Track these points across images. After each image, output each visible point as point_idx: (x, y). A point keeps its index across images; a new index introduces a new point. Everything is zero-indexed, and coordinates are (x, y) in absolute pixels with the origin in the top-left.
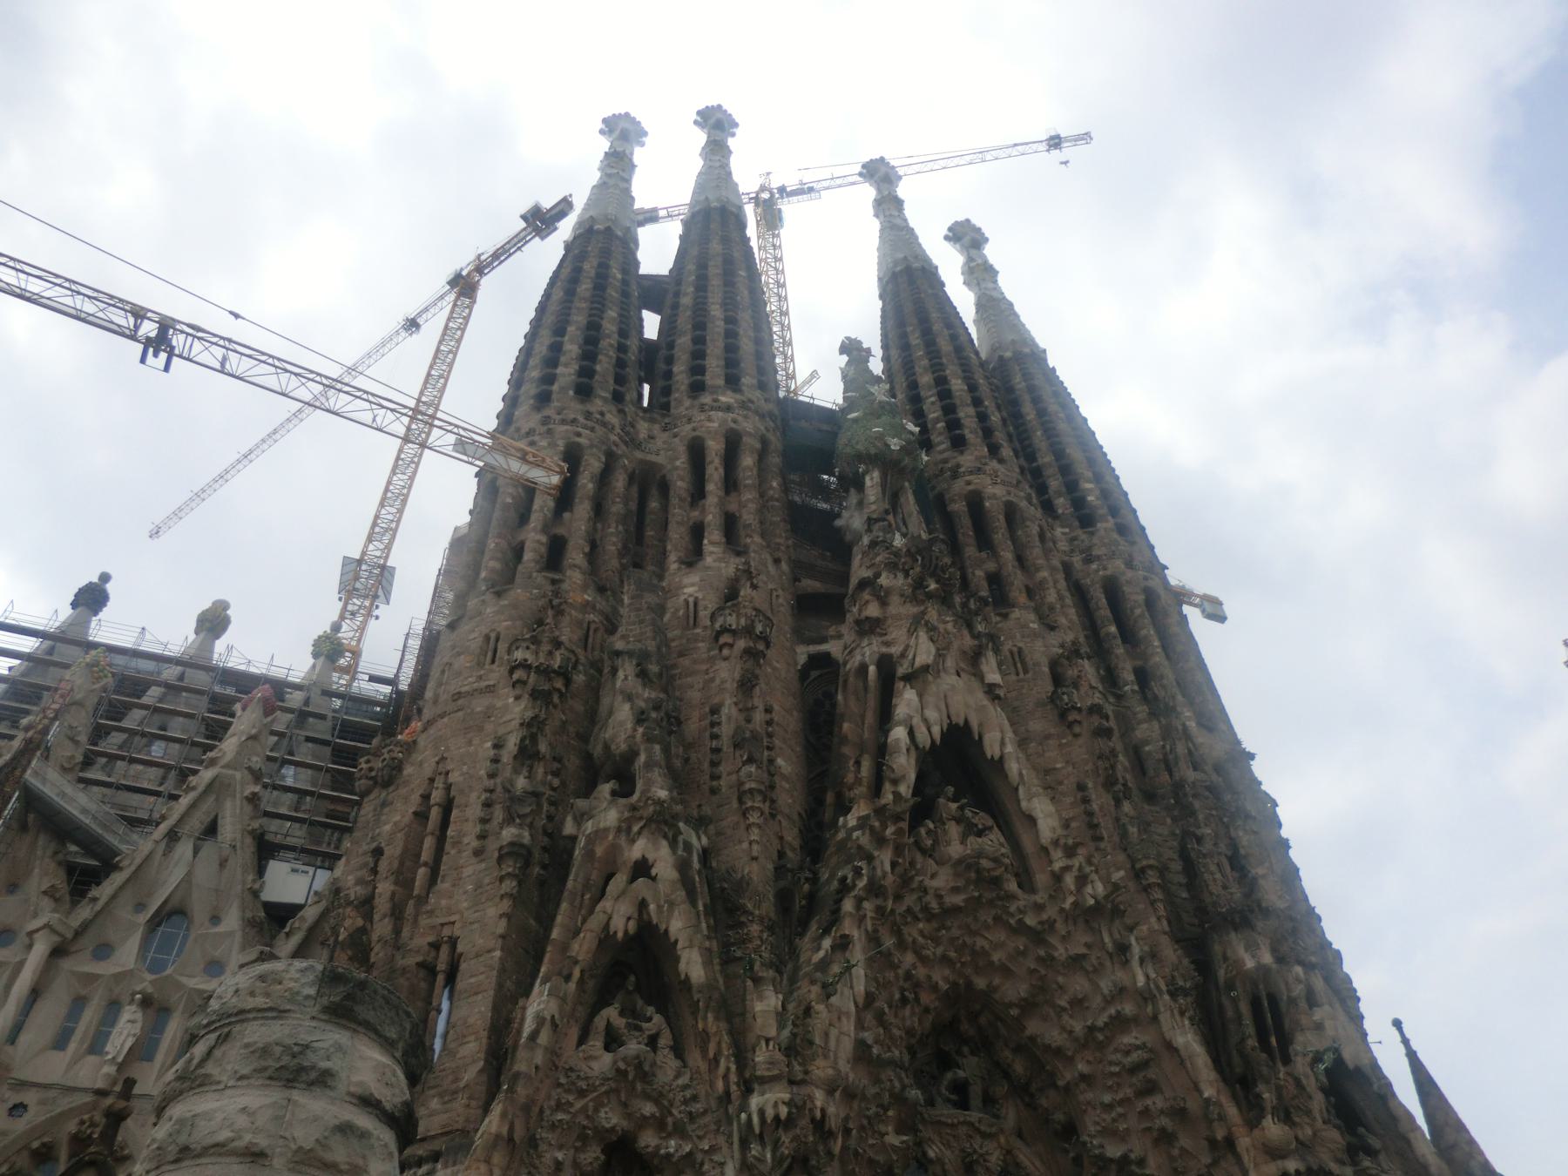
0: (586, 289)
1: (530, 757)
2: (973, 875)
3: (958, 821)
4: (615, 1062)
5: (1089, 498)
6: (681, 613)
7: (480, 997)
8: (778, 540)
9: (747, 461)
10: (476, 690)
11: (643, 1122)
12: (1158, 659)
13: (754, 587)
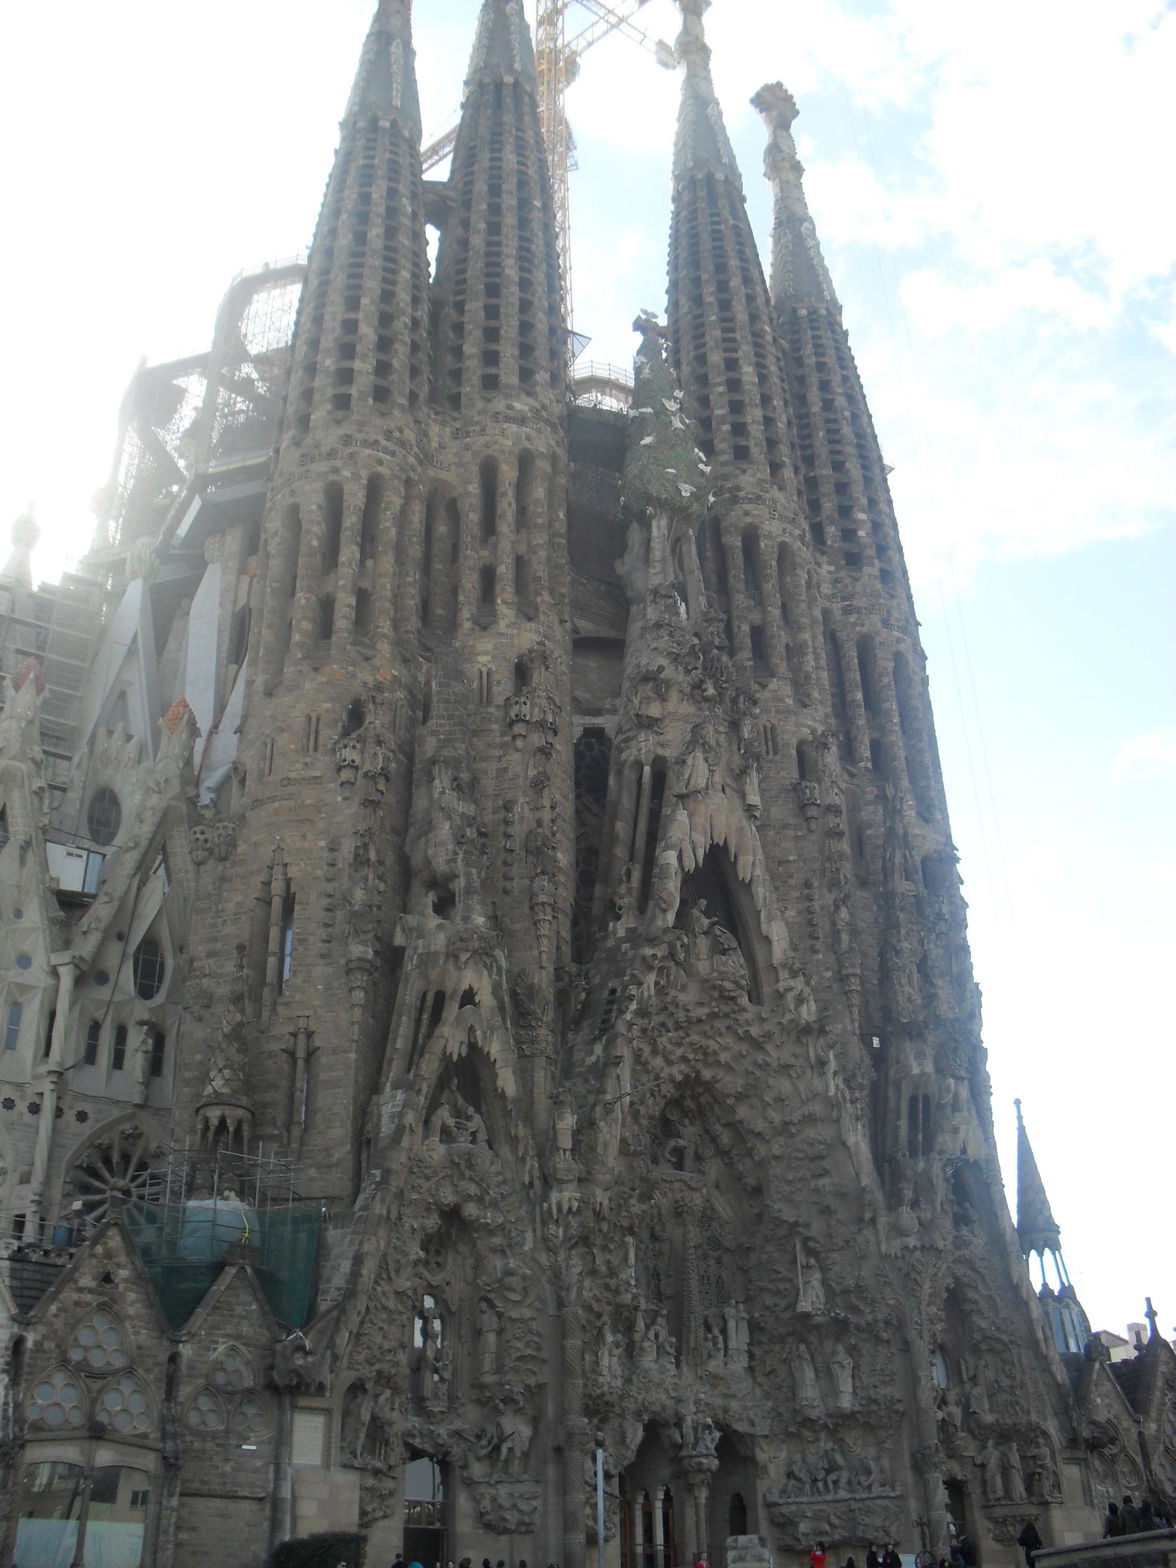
0: (378, 236)
1: (362, 863)
2: (716, 994)
3: (704, 933)
4: (450, 1155)
5: (861, 533)
6: (475, 685)
7: (341, 1090)
8: (564, 590)
9: (539, 492)
10: (304, 779)
11: (469, 1198)
12: (895, 736)
13: (547, 668)
